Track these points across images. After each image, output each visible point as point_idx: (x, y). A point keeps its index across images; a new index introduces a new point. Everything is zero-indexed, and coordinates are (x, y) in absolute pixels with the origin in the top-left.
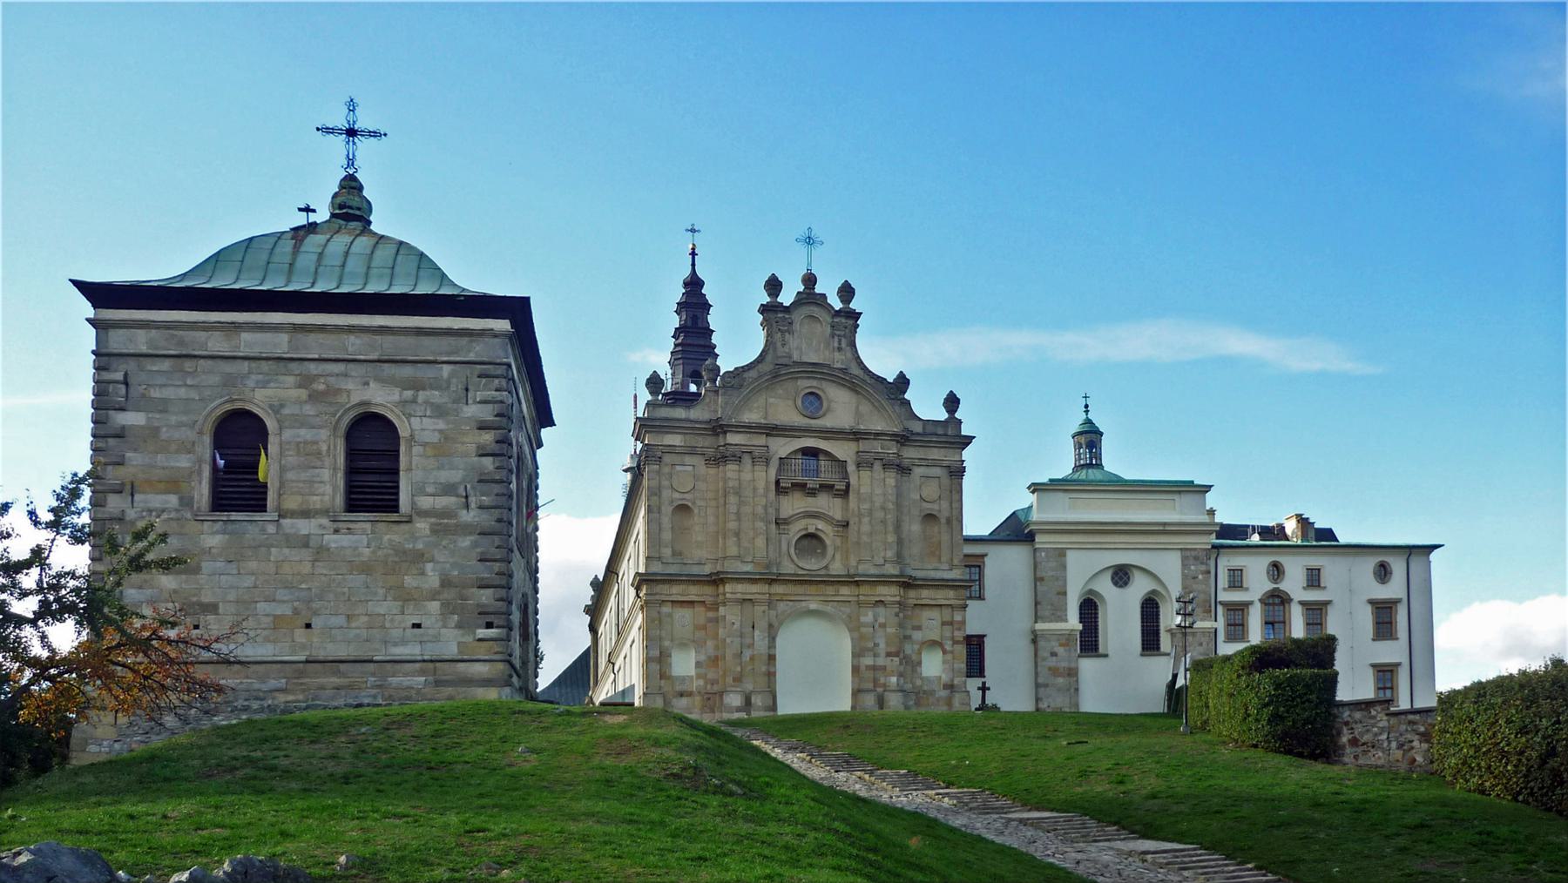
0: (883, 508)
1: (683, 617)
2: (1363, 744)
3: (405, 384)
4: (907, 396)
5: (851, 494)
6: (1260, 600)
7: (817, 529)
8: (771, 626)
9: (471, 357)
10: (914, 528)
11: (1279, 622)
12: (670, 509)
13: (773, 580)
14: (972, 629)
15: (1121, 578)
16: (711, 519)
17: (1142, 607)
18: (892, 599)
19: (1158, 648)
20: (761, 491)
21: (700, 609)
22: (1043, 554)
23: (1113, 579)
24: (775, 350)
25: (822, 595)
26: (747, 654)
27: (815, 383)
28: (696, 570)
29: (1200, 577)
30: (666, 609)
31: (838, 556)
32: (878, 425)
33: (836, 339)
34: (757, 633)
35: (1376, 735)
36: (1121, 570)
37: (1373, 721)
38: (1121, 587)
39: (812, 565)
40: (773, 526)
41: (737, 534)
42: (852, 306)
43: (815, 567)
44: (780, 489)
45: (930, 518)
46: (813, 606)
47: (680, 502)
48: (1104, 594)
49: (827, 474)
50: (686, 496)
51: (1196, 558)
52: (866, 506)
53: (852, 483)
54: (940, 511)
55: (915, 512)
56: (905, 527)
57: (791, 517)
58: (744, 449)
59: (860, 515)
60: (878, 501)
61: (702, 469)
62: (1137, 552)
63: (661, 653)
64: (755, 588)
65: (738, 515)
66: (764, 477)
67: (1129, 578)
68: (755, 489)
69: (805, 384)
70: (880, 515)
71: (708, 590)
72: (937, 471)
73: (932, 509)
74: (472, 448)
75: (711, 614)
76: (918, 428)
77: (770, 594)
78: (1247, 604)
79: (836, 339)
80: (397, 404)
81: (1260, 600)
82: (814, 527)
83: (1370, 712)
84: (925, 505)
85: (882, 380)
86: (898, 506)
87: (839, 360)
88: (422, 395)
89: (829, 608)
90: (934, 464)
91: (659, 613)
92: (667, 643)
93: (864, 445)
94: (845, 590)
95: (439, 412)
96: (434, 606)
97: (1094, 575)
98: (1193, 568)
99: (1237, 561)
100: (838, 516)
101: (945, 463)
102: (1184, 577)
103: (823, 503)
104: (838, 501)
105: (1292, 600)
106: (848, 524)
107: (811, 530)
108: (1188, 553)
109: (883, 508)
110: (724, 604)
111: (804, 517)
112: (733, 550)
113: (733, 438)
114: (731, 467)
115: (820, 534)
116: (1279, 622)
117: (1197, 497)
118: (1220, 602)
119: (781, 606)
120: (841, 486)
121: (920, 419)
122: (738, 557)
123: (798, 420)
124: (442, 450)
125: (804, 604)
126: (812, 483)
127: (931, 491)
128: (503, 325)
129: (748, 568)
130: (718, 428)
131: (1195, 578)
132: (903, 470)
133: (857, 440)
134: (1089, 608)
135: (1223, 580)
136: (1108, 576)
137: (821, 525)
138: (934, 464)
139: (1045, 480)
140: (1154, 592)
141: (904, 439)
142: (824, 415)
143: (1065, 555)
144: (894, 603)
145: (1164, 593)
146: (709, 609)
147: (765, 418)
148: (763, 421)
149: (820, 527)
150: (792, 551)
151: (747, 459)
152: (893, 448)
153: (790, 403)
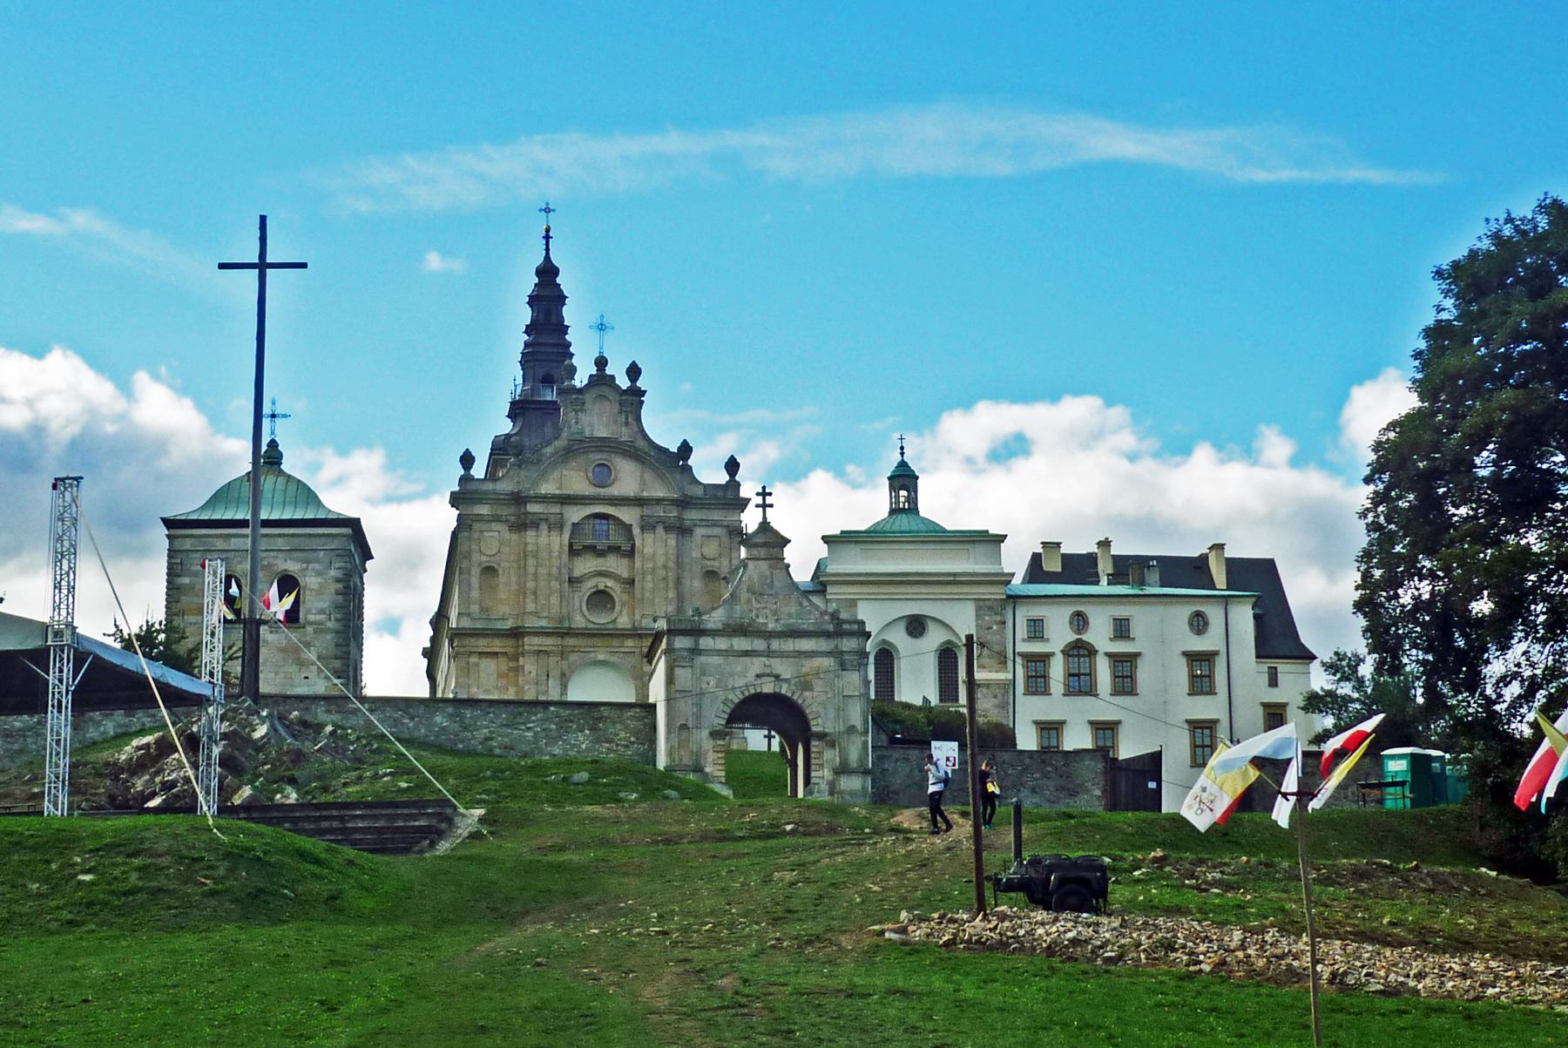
4: (690, 462)
6: (1062, 651)
7: (606, 586)
8: (563, 675)
10: (695, 584)
12: (479, 570)
15: (915, 628)
16: (514, 579)
19: (957, 700)
21: (503, 660)
23: (907, 629)
25: (611, 647)
27: (604, 456)
28: (499, 625)
30: (473, 659)
31: (625, 611)
32: (660, 492)
33: (623, 416)
38: (916, 637)
39: (601, 619)
40: (567, 585)
41: (535, 593)
42: (638, 384)
43: (602, 621)
44: (573, 552)
45: (711, 574)
46: (601, 657)
47: (487, 564)
49: (616, 538)
50: (492, 558)
51: (991, 608)
52: (650, 565)
53: (637, 544)
54: (719, 568)
55: (697, 569)
56: (687, 583)
58: (542, 516)
59: (644, 574)
60: (661, 561)
61: (507, 535)
62: (939, 602)
64: (550, 641)
65: (536, 574)
66: (557, 542)
68: (551, 552)
69: (598, 457)
70: (662, 573)
71: (510, 642)
72: (717, 531)
73: (713, 566)
74: (333, 591)
75: (512, 664)
76: (699, 492)
78: (1052, 654)
81: (1062, 651)
86: (679, 565)
87: (625, 435)
89: (613, 659)
90: (715, 524)
91: (468, 663)
93: (647, 511)
94: (630, 643)
95: (319, 574)
97: (887, 625)
98: (987, 618)
99: (1037, 611)
100: (625, 575)
101: (725, 523)
103: (614, 564)
104: (625, 561)
106: (634, 581)
107: (601, 587)
108: (981, 603)
109: (665, 567)
110: (523, 656)
111: (595, 576)
112: (531, 607)
113: (532, 508)
114: (530, 535)
115: (608, 590)
117: (990, 547)
119: (573, 657)
121: (701, 484)
122: (536, 614)
124: (319, 592)
125: (593, 655)
126: (602, 544)
127: (711, 549)
129: (543, 623)
130: (519, 499)
132: (683, 531)
133: (642, 505)
136: (902, 627)
137: (610, 583)
138: (715, 524)
139: (837, 532)
140: (949, 642)
141: (684, 503)
143: (856, 606)
146: (510, 660)
147: (560, 489)
148: (557, 492)
149: (609, 585)
150: (584, 608)
151: (544, 526)
152: (673, 513)
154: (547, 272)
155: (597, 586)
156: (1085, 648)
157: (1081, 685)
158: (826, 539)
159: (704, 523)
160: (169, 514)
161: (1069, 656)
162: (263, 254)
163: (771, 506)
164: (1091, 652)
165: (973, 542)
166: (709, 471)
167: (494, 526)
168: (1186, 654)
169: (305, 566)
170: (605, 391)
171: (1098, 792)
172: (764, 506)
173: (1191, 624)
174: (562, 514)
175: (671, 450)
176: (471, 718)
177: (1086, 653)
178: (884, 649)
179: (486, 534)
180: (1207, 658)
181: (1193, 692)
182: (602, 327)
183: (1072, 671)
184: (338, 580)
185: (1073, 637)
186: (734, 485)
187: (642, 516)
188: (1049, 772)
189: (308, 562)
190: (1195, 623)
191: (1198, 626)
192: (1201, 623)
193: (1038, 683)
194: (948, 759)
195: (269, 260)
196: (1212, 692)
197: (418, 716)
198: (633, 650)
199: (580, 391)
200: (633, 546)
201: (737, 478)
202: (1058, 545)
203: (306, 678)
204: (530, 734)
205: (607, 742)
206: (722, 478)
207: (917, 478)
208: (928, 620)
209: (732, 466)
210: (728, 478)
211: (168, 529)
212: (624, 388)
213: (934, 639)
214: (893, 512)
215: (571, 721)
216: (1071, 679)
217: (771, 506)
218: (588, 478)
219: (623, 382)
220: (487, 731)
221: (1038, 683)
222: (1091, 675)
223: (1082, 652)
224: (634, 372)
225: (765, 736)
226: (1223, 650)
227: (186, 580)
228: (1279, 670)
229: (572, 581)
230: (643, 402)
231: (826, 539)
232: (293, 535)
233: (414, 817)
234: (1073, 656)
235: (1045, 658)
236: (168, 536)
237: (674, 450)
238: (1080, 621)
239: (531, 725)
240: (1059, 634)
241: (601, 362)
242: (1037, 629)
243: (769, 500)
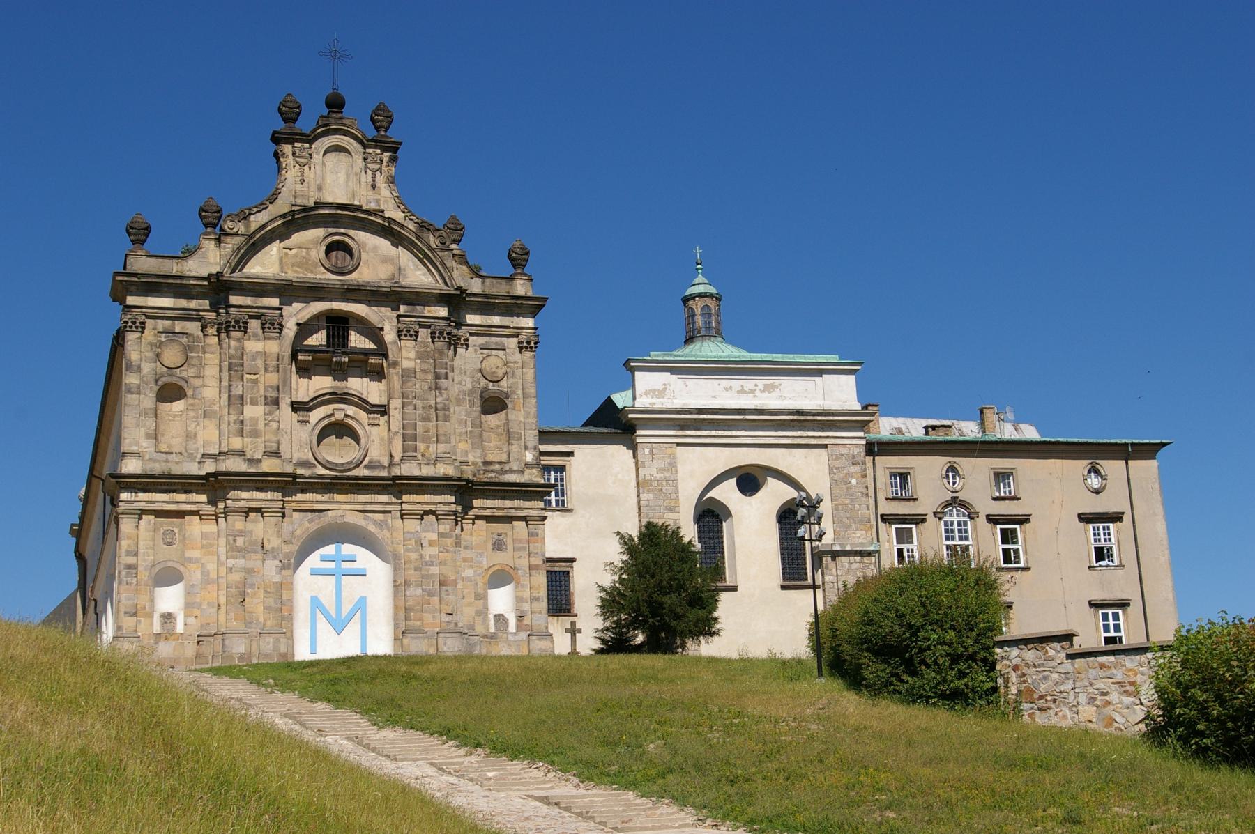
2: (1041, 697)
7: (346, 416)
14: (554, 549)
18: (447, 508)
22: (647, 451)
33: (369, 172)
35: (1056, 684)
37: (1053, 664)
58: (253, 312)
66: (277, 347)
83: (1047, 652)
107: (339, 416)
115: (348, 421)
136: (732, 482)
137: (351, 410)
144: (447, 514)
149: (349, 413)
155: (332, 415)
165: (820, 373)
198: (388, 508)
213: (775, 494)
225: (567, 631)
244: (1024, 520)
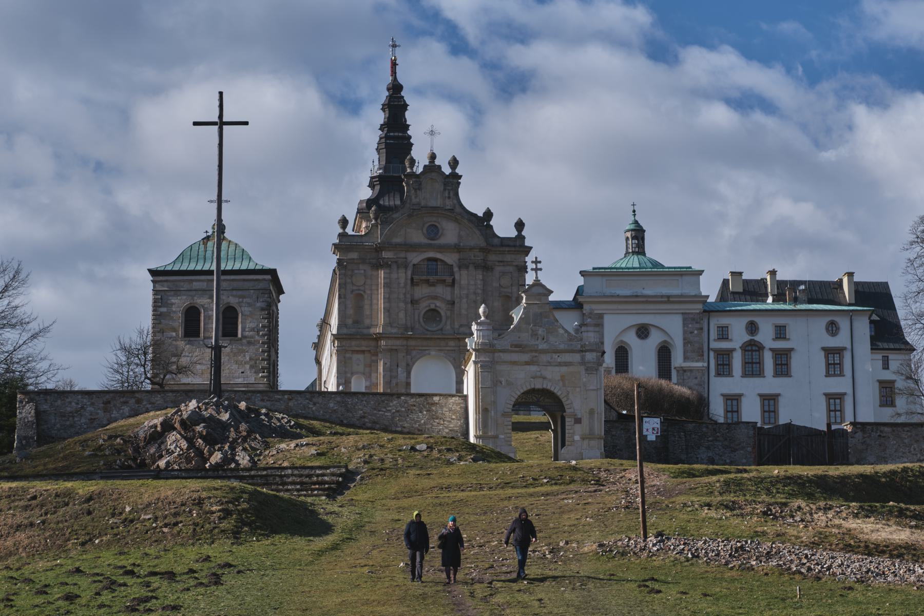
0: (475, 293)
1: (359, 361)
3: (240, 297)
5: (456, 285)
6: (740, 347)
7: (436, 306)
8: (408, 365)
9: (259, 287)
11: (756, 363)
13: (408, 338)
15: (643, 333)
17: (659, 352)
20: (402, 285)
23: (637, 333)
24: (411, 200)
26: (394, 381)
29: (696, 332)
31: (448, 323)
33: (447, 192)
34: (400, 369)
36: (643, 327)
38: (643, 338)
40: (410, 305)
48: (628, 342)
51: (693, 319)
52: (465, 292)
54: (511, 293)
57: (422, 298)
63: (345, 381)
64: (398, 342)
66: (402, 276)
67: (648, 333)
68: (399, 284)
72: (511, 269)
77: (407, 346)
78: (734, 350)
79: (447, 192)
80: (237, 303)
81: (740, 347)
82: (434, 305)
84: (502, 289)
85: (475, 215)
87: (449, 204)
88: (245, 300)
91: (345, 357)
92: (349, 375)
94: (452, 343)
95: (249, 305)
96: (248, 367)
98: (690, 326)
99: (724, 321)
100: (449, 298)
102: (685, 332)
103: (440, 290)
104: (449, 289)
105: (764, 347)
107: (433, 306)
109: (475, 293)
113: (385, 255)
116: (756, 363)
118: (711, 349)
120: (449, 280)
121: (499, 237)
123: (424, 240)
128: (269, 277)
129: (394, 331)
131: (692, 333)
132: (486, 268)
134: (622, 354)
135: (714, 334)
137: (438, 303)
140: (665, 342)
142: (440, 237)
143: (602, 318)
145: (671, 342)
149: (438, 304)
150: (421, 320)
151: (394, 267)
153: (420, 231)
154: (396, 88)
156: (756, 346)
157: (753, 369)
158: (583, 273)
159: (502, 264)
160: (153, 266)
161: (746, 351)
162: (221, 116)
163: (541, 269)
164: (760, 348)
166: (503, 228)
167: (361, 267)
168: (824, 349)
169: (241, 300)
170: (434, 175)
171: (749, 449)
172: (536, 270)
173: (827, 329)
174: (406, 258)
175: (479, 215)
176: (352, 404)
177: (757, 349)
178: (622, 346)
179: (356, 271)
180: (839, 351)
181: (828, 375)
182: (432, 133)
183: (747, 361)
184: (263, 309)
185: (747, 338)
186: (520, 237)
187: (459, 259)
188: (718, 437)
189: (243, 297)
190: (830, 329)
191: (832, 330)
192: (834, 329)
193: (724, 369)
194: (653, 429)
195: (225, 120)
196: (841, 375)
197: (318, 403)
199: (418, 176)
200: (454, 280)
201: (523, 233)
202: (740, 274)
203: (243, 373)
204: (389, 414)
205: (437, 419)
206: (513, 233)
207: (644, 231)
208: (650, 327)
209: (520, 225)
210: (516, 233)
211: (152, 276)
212: (447, 173)
213: (655, 339)
214: (627, 253)
215: (415, 406)
216: (747, 365)
217: (541, 269)
218: (423, 234)
219: (447, 170)
220: (361, 412)
221: (724, 369)
222: (760, 363)
223: (754, 348)
224: (454, 163)
226: (849, 346)
227: (164, 310)
228: (890, 358)
229: (414, 302)
230: (460, 183)
231: (583, 273)
232: (233, 280)
233: (323, 475)
234: (748, 351)
235: (729, 353)
236: (152, 281)
237: (480, 214)
238: (752, 328)
239: (390, 408)
240: (739, 335)
241: (433, 157)
242: (724, 333)
243: (539, 266)
244: (792, 349)
